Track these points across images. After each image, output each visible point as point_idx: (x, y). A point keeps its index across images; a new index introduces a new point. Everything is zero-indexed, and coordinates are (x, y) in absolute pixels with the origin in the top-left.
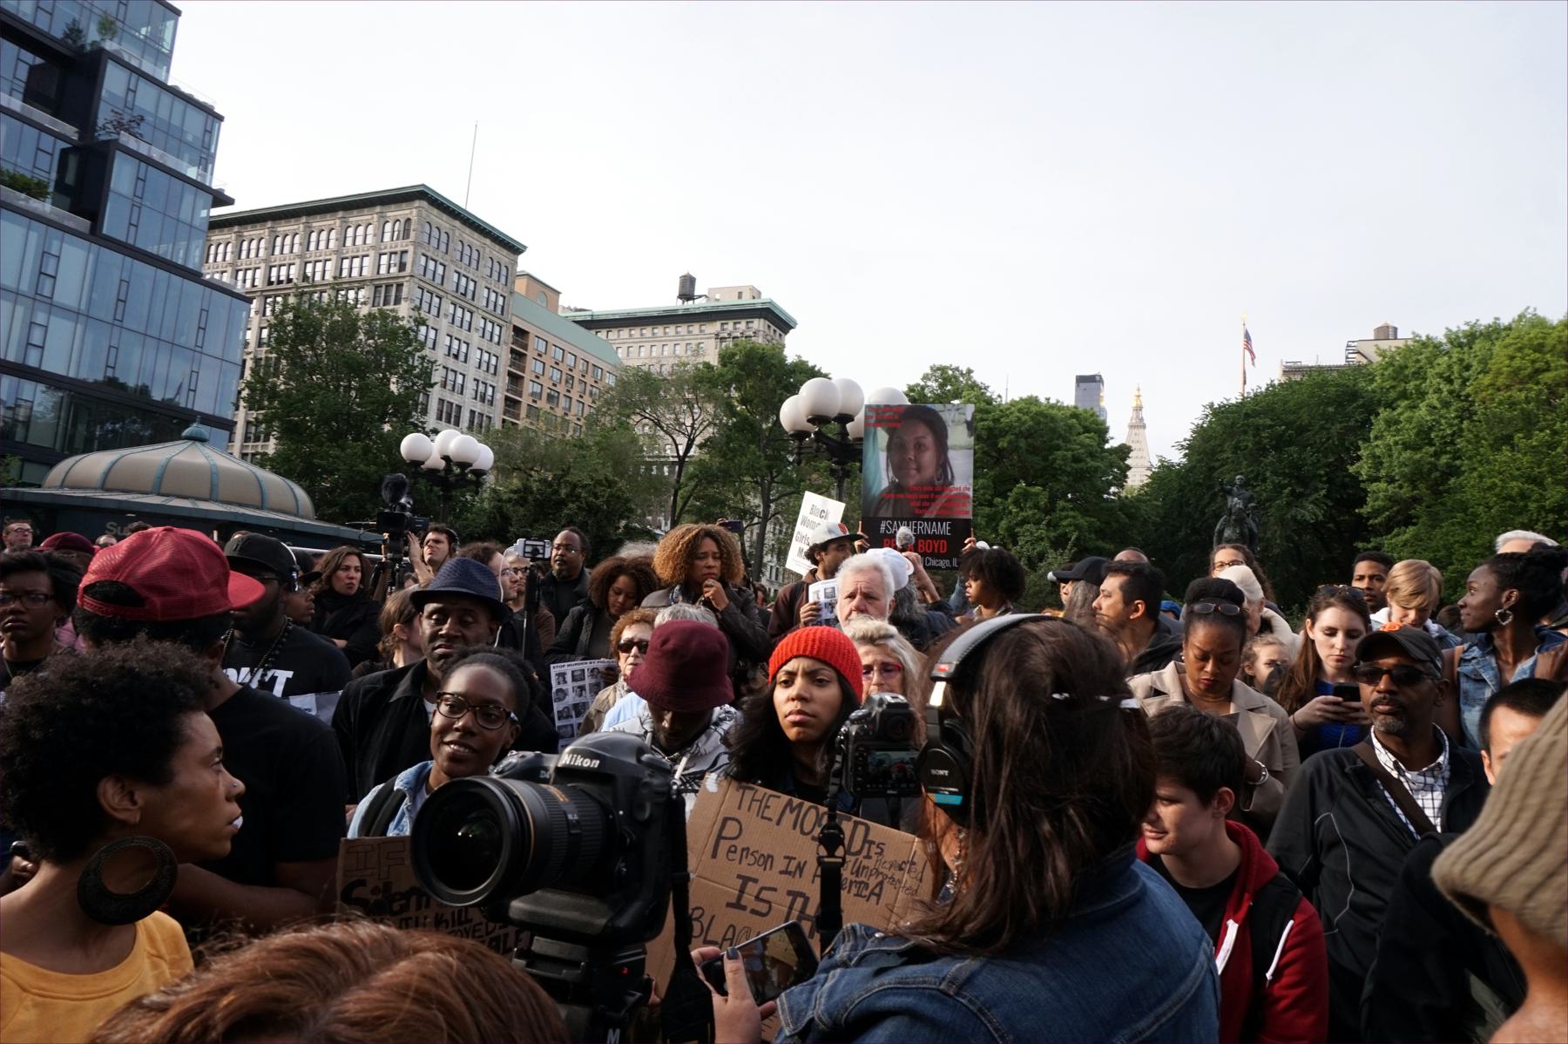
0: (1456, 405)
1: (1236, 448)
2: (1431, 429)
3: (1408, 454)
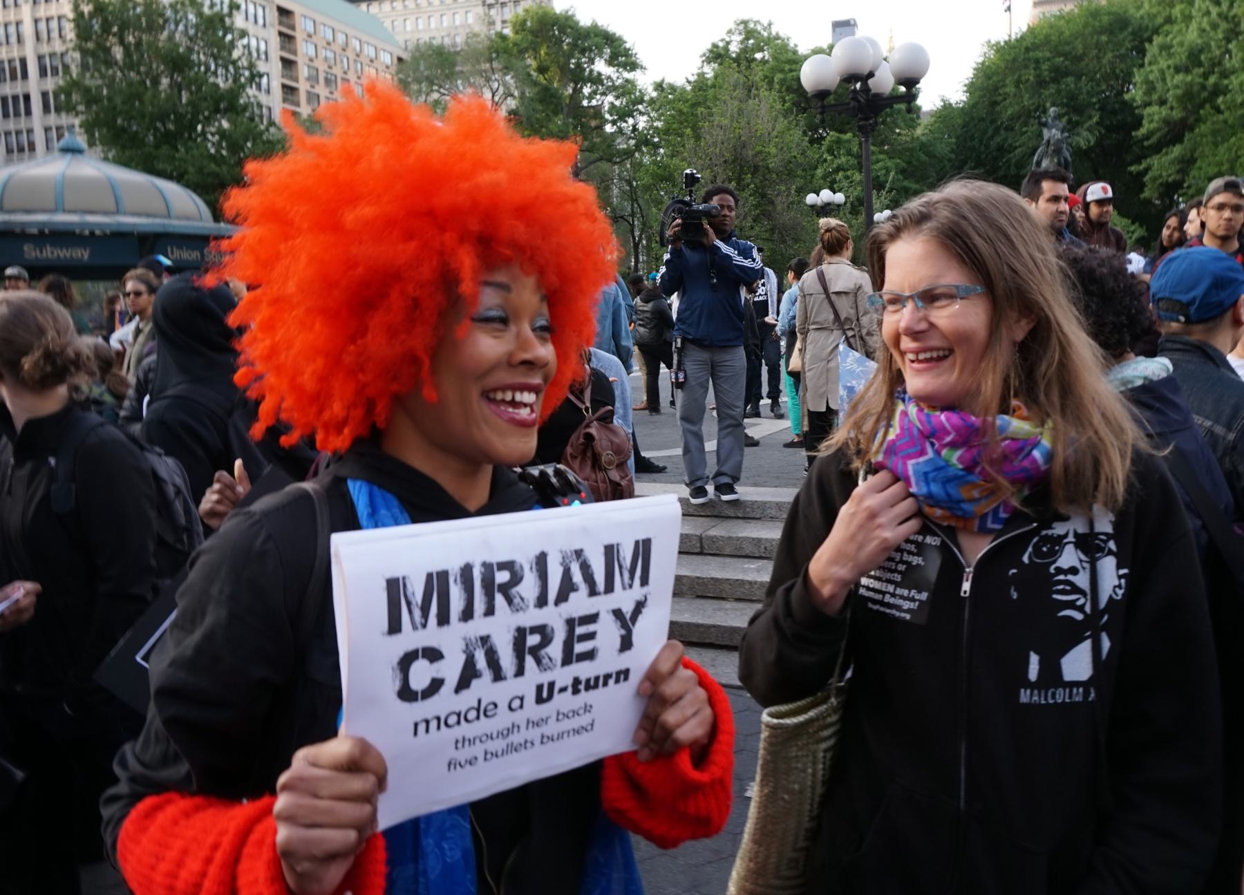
0: (1224, 25)
1: (1018, 83)
2: (1201, 51)
3: (1179, 78)
